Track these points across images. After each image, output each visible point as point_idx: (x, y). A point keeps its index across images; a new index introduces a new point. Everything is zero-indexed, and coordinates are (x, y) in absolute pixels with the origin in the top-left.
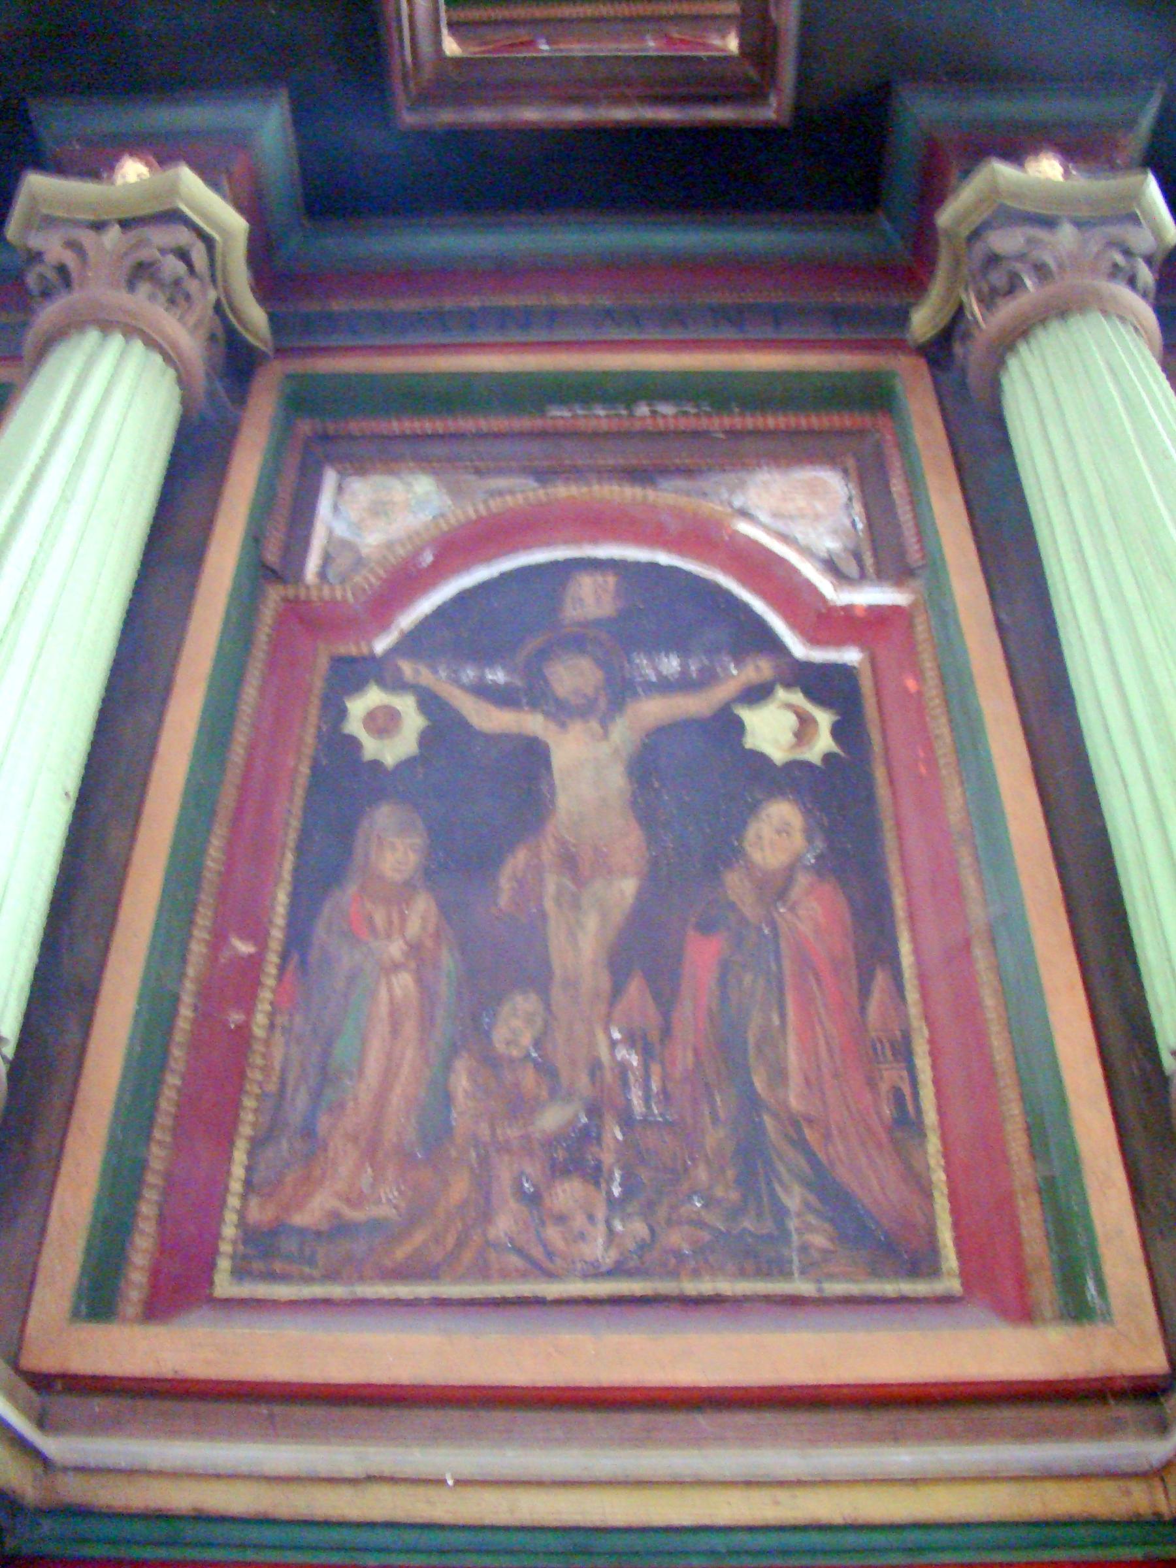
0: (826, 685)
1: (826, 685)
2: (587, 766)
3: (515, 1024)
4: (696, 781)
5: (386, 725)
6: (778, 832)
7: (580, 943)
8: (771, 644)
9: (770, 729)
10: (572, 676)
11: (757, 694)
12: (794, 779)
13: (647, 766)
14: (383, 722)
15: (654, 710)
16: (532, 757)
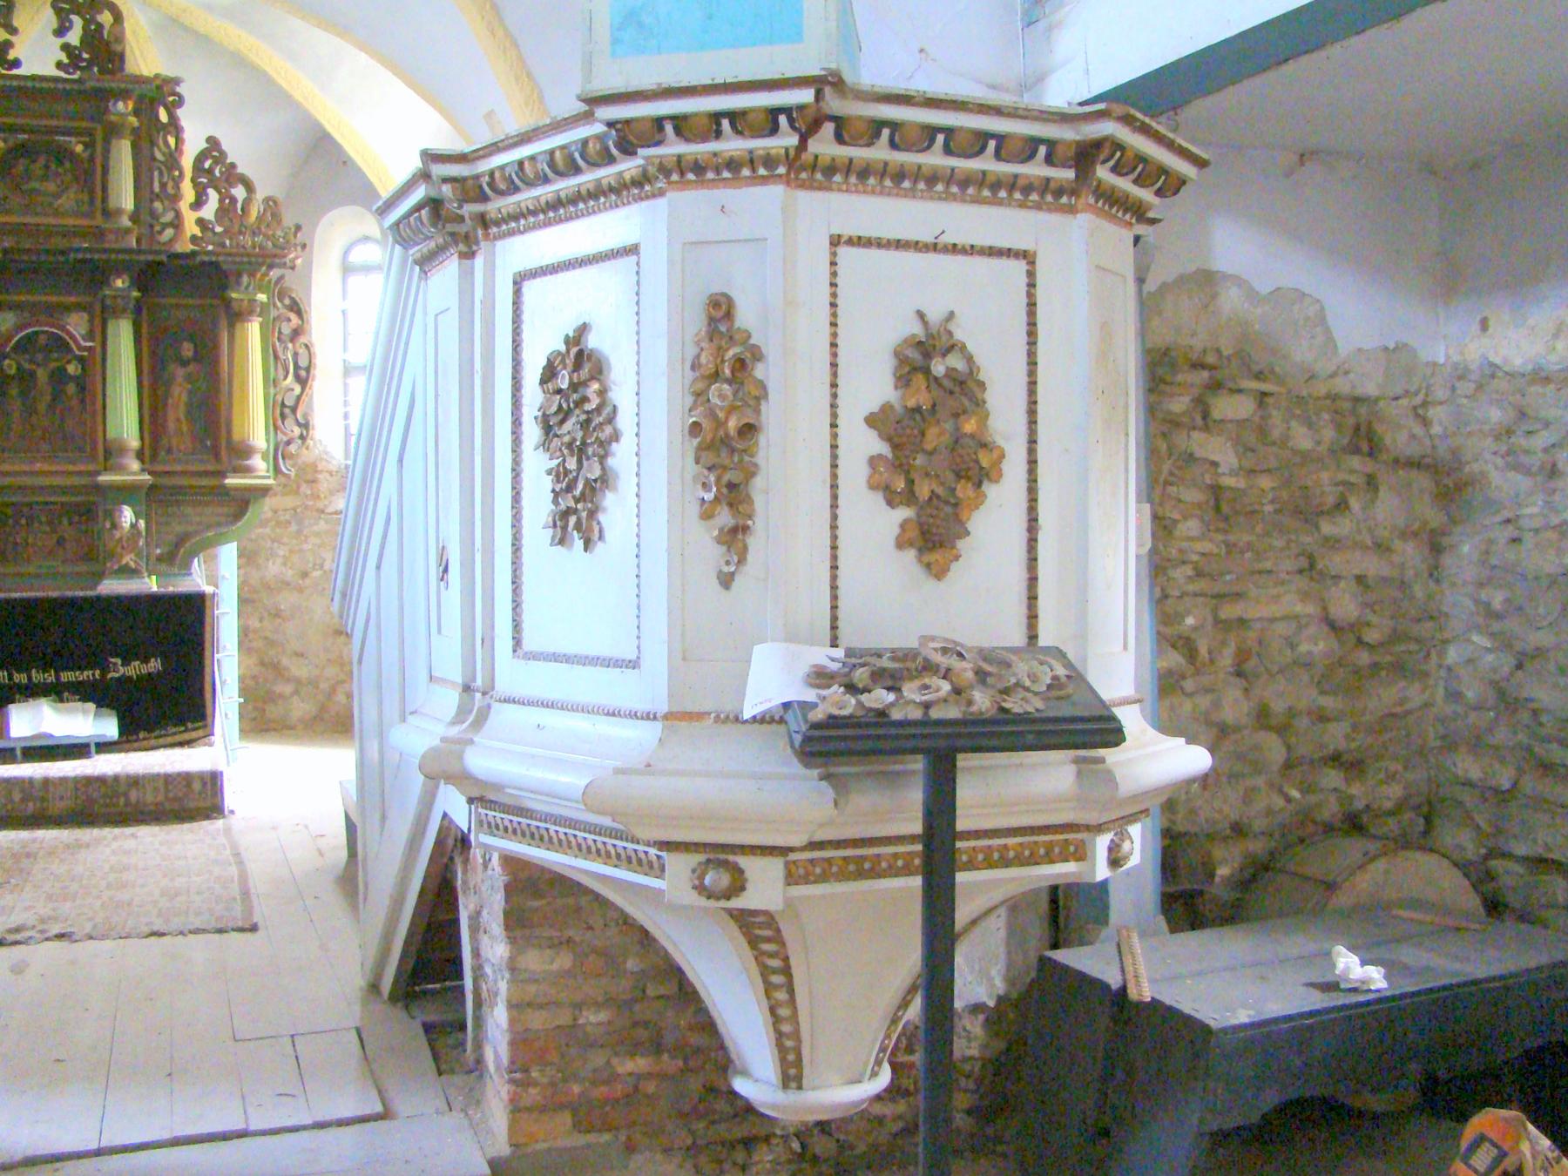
0: (81, 360)
1: (81, 360)
2: (42, 375)
3: (34, 419)
4: (59, 377)
5: (10, 367)
6: (71, 388)
7: (42, 407)
8: (70, 350)
9: (72, 369)
10: (39, 357)
11: (69, 362)
12: (74, 378)
13: (52, 375)
14: (10, 366)
15: (53, 365)
16: (32, 374)
